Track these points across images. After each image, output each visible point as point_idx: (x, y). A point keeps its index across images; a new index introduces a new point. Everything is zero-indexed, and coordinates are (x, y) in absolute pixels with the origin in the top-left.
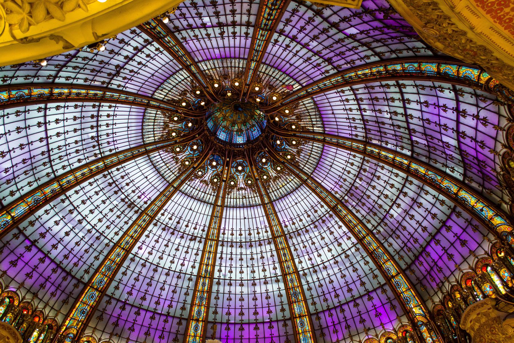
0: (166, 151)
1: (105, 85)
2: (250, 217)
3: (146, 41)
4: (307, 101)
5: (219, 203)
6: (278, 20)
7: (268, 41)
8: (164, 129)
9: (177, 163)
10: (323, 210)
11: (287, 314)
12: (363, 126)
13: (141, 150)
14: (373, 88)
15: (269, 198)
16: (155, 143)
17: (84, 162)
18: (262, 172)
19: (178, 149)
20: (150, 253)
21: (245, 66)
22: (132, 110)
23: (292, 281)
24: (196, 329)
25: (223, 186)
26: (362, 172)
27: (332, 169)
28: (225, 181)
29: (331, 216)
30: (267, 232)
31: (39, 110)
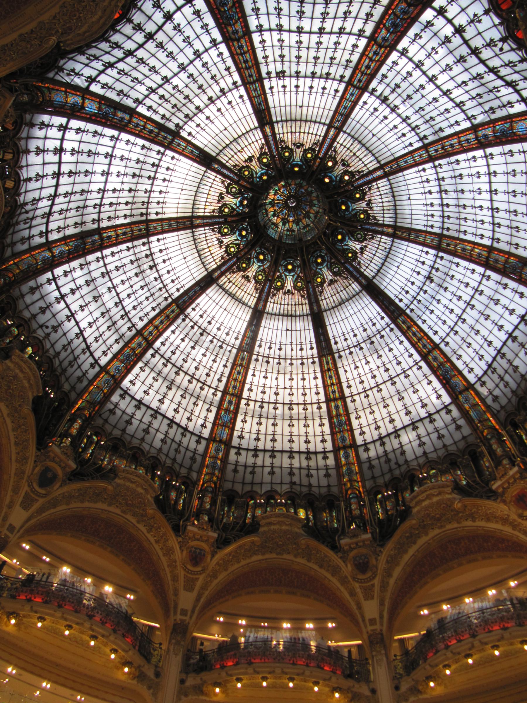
0: (213, 230)
2: (294, 329)
3: (235, 83)
4: (383, 183)
6: (372, 76)
7: (355, 103)
10: (383, 323)
11: (329, 446)
12: (441, 213)
16: (204, 217)
19: (226, 230)
21: (323, 134)
23: (337, 407)
24: (217, 450)
26: (434, 271)
28: (270, 281)
29: (392, 330)
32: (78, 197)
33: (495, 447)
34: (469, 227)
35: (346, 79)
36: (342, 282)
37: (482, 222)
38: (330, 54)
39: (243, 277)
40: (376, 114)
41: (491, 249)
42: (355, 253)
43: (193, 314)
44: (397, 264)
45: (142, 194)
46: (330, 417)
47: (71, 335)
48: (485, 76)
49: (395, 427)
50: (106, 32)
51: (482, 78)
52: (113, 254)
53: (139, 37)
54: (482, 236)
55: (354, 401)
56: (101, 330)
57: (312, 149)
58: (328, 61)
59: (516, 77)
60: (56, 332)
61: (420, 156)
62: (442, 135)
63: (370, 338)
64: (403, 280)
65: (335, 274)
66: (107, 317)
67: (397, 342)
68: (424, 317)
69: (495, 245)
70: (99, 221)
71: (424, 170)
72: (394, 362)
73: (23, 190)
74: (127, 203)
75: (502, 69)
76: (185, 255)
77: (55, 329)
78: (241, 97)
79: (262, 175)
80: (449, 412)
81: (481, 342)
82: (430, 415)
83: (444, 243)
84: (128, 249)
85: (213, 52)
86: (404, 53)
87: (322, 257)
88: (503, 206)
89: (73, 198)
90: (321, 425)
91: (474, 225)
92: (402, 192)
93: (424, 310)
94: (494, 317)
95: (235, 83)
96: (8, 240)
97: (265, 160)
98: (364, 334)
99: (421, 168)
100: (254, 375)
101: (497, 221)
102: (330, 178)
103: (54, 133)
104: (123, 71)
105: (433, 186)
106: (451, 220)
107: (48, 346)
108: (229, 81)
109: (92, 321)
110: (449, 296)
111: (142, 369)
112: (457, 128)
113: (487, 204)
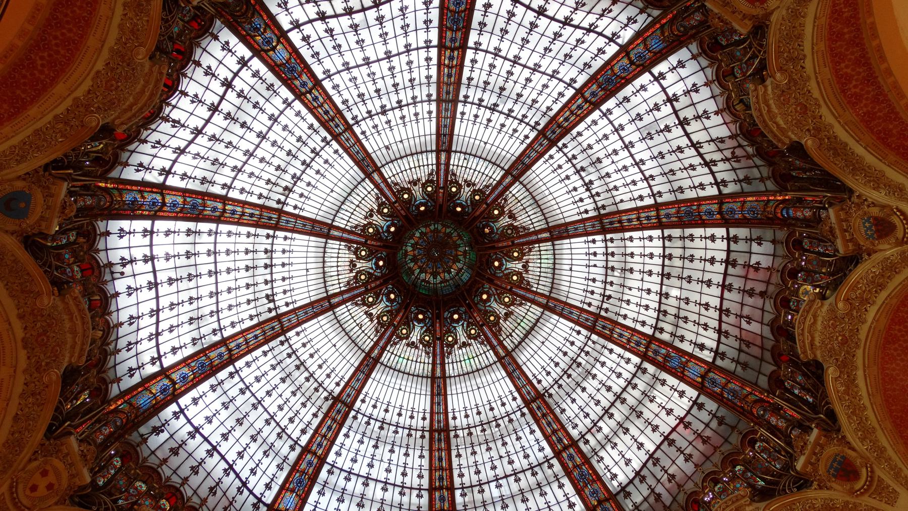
0: (357, 304)
1: (280, 206)
4: (516, 189)
5: (438, 373)
6: (458, 83)
7: (453, 118)
8: (351, 271)
9: (372, 320)
13: (323, 306)
14: (580, 134)
15: (504, 348)
17: (255, 321)
18: (486, 313)
19: (371, 299)
20: (354, 461)
22: (311, 244)
23: (571, 457)
25: (439, 346)
27: (574, 274)
30: (514, 399)
31: (210, 233)
32: (187, 307)
33: (773, 421)
34: (623, 194)
35: (434, 97)
36: (519, 311)
37: (634, 183)
38: (407, 77)
39: (408, 345)
40: (478, 120)
41: (657, 206)
42: (519, 274)
43: (363, 407)
44: (568, 267)
45: (262, 287)
46: (568, 473)
47: (218, 473)
48: (563, 31)
49: (648, 452)
50: (160, 109)
51: (561, 35)
52: (248, 364)
53: (204, 112)
54: (641, 198)
55: (587, 442)
56: (257, 458)
57: (429, 182)
58: (408, 84)
59: (591, 18)
60: (197, 473)
61: (541, 145)
62: (552, 113)
63: (575, 361)
64: (583, 281)
65: (507, 306)
66: (260, 440)
67: (606, 352)
68: (623, 312)
69: (659, 200)
70: (221, 329)
71: (551, 157)
72: (614, 377)
73: (113, 308)
74: (249, 302)
75: (573, 16)
76: (334, 341)
77: (195, 470)
78: (336, 152)
79: (389, 227)
80: (701, 407)
81: (696, 309)
82: (681, 420)
83: (607, 223)
84: (265, 353)
85: (289, 112)
86: (477, 48)
87: (487, 293)
88: (646, 155)
89: (182, 309)
90: (561, 486)
91: (627, 190)
92: (541, 190)
93: (619, 304)
94: (696, 275)
95: (324, 140)
96: (111, 374)
97: (386, 211)
98: (567, 359)
99: (547, 156)
100: (459, 456)
101: (647, 174)
102: (460, 205)
103: (138, 240)
104: (198, 154)
105: (568, 169)
106: (603, 196)
107: (189, 492)
108: (318, 139)
109: (241, 449)
110: (639, 276)
111: (321, 493)
112: (564, 100)
113: (629, 162)
